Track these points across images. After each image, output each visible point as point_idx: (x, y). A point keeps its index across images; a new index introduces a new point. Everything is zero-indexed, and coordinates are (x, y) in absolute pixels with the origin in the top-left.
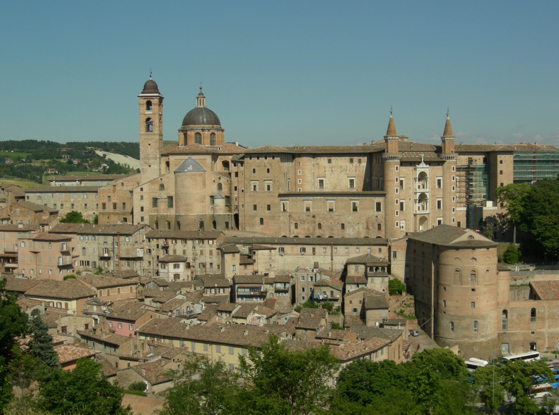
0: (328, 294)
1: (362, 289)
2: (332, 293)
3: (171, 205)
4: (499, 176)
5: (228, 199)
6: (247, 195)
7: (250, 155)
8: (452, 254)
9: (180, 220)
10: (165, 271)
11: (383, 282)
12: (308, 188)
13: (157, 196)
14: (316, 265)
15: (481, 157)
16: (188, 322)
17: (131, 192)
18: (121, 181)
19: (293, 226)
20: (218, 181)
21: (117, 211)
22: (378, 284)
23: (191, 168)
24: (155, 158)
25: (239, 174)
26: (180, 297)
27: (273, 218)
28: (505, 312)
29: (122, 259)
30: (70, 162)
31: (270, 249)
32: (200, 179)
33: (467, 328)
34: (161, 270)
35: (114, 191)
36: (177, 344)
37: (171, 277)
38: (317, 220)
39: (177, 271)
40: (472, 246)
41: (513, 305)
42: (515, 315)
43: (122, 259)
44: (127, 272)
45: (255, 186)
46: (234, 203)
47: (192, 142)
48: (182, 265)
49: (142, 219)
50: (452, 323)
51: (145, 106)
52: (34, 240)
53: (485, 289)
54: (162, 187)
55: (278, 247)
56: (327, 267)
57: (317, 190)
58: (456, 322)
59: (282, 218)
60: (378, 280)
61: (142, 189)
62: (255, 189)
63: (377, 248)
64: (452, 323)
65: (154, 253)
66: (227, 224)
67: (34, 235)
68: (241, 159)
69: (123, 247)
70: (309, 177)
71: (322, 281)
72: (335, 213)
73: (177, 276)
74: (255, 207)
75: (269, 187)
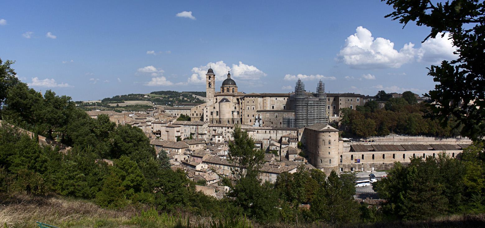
0: (275, 148)
1: (287, 147)
2: (276, 148)
3: (217, 115)
4: (340, 105)
5: (238, 112)
6: (245, 111)
7: (247, 96)
8: (322, 134)
9: (221, 120)
10: (215, 139)
11: (295, 144)
12: (268, 109)
13: (212, 111)
14: (270, 137)
15: (333, 98)
16: (222, 158)
17: (203, 110)
18: (199, 105)
20: (235, 106)
21: (198, 116)
22: (294, 145)
24: (212, 97)
25: (243, 103)
26: (219, 148)
28: (341, 156)
29: (199, 134)
30: (183, 99)
31: (254, 131)
32: (228, 105)
33: (326, 162)
34: (213, 138)
35: (197, 109)
36: (218, 166)
37: (217, 141)
38: (271, 121)
39: (219, 139)
40: (329, 131)
41: (344, 153)
42: (345, 157)
43: (199, 134)
44: (201, 139)
47: (225, 91)
48: (221, 137)
49: (207, 119)
50: (321, 160)
51: (208, 78)
52: (167, 127)
53: (334, 147)
54: (214, 108)
55: (256, 130)
56: (274, 138)
57: (271, 109)
58: (323, 160)
60: (293, 143)
61: (207, 109)
63: (293, 131)
64: (321, 160)
65: (211, 132)
66: (238, 121)
67: (167, 125)
68: (243, 98)
69: (199, 130)
70: (269, 105)
71: (273, 143)
72: (278, 118)
73: (219, 141)
75: (253, 108)
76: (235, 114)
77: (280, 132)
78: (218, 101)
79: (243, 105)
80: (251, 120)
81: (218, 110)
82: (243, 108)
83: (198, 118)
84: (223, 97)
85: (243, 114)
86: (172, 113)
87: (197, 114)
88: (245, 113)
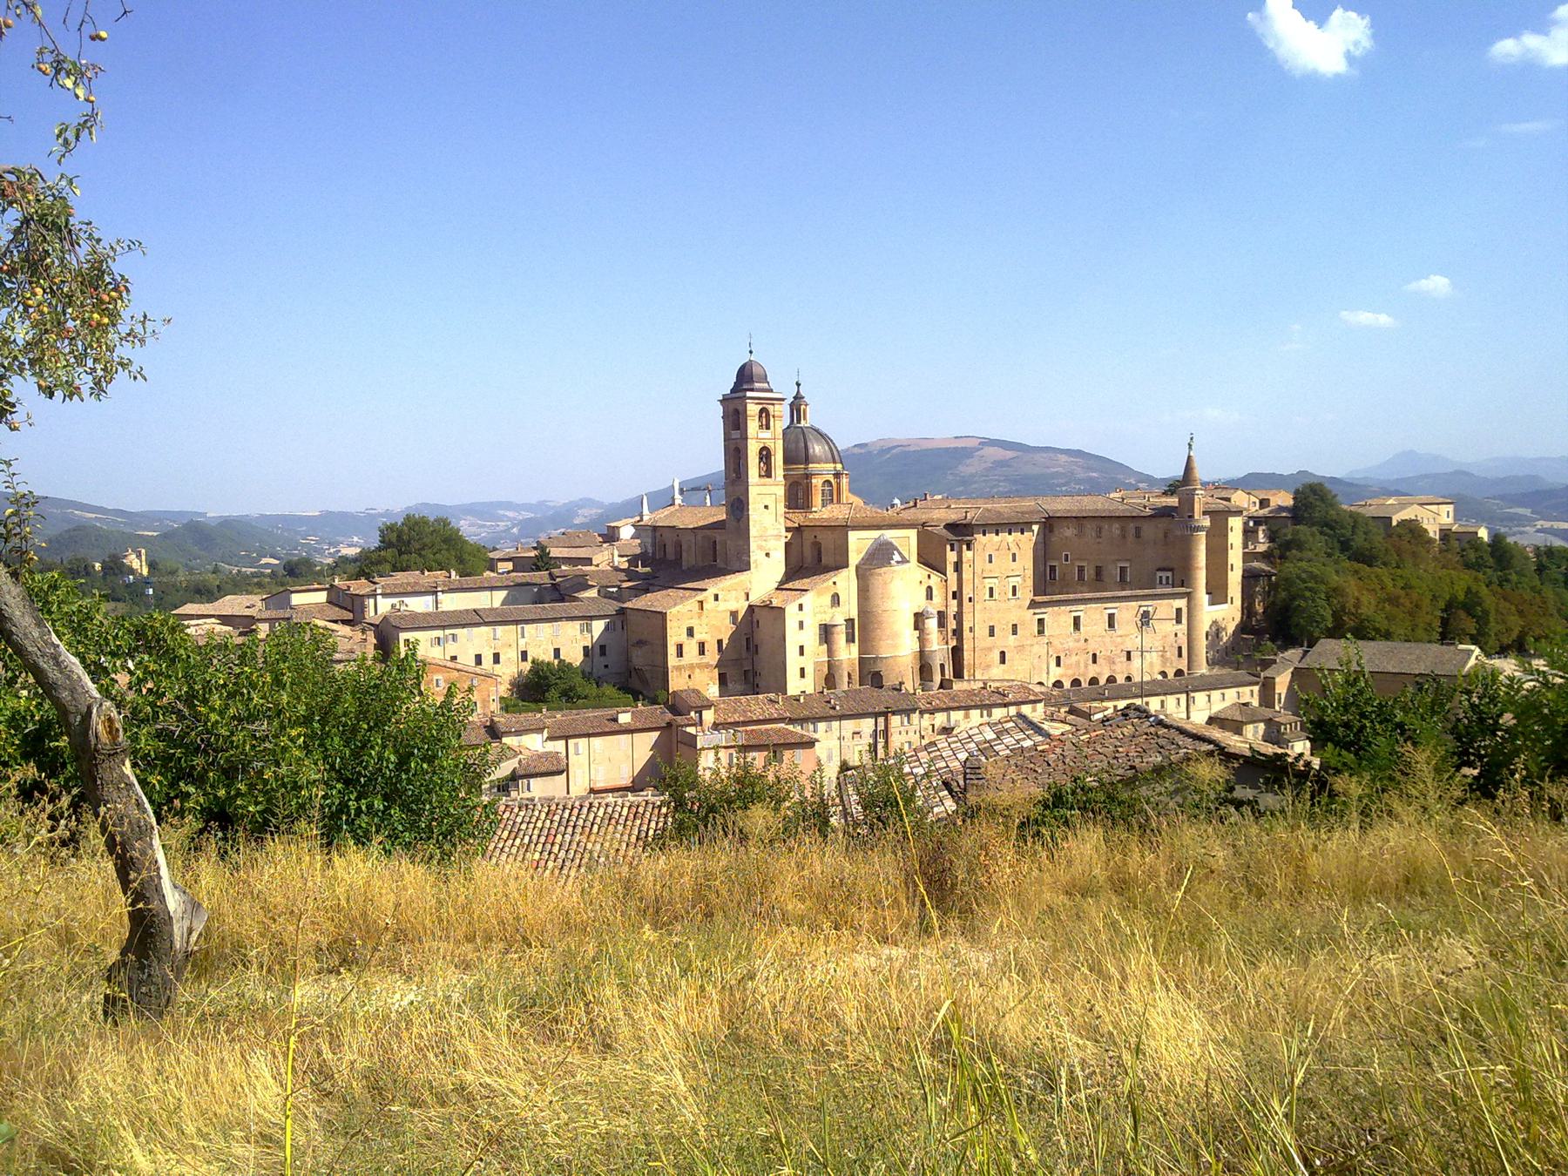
3: (850, 639)
5: (942, 616)
13: (827, 620)
18: (712, 591)
19: (1053, 663)
23: (897, 557)
25: (965, 566)
27: (1020, 648)
38: (1093, 647)
45: (991, 589)
46: (952, 624)
54: (836, 600)
59: (1036, 649)
61: (801, 607)
62: (991, 595)
66: (942, 666)
74: (992, 633)
76: (932, 624)
77: (1200, 697)
78: (854, 558)
79: (967, 575)
80: (1003, 653)
81: (854, 614)
82: (967, 592)
83: (707, 666)
84: (875, 534)
85: (966, 626)
86: (452, 649)
87: (702, 646)
88: (977, 618)
